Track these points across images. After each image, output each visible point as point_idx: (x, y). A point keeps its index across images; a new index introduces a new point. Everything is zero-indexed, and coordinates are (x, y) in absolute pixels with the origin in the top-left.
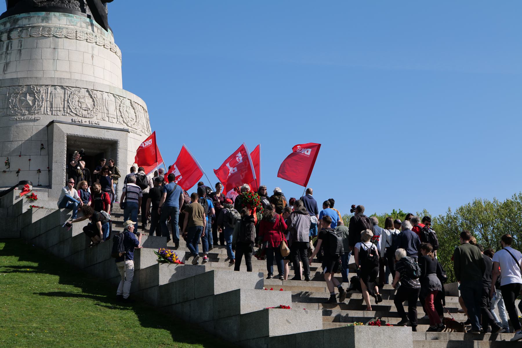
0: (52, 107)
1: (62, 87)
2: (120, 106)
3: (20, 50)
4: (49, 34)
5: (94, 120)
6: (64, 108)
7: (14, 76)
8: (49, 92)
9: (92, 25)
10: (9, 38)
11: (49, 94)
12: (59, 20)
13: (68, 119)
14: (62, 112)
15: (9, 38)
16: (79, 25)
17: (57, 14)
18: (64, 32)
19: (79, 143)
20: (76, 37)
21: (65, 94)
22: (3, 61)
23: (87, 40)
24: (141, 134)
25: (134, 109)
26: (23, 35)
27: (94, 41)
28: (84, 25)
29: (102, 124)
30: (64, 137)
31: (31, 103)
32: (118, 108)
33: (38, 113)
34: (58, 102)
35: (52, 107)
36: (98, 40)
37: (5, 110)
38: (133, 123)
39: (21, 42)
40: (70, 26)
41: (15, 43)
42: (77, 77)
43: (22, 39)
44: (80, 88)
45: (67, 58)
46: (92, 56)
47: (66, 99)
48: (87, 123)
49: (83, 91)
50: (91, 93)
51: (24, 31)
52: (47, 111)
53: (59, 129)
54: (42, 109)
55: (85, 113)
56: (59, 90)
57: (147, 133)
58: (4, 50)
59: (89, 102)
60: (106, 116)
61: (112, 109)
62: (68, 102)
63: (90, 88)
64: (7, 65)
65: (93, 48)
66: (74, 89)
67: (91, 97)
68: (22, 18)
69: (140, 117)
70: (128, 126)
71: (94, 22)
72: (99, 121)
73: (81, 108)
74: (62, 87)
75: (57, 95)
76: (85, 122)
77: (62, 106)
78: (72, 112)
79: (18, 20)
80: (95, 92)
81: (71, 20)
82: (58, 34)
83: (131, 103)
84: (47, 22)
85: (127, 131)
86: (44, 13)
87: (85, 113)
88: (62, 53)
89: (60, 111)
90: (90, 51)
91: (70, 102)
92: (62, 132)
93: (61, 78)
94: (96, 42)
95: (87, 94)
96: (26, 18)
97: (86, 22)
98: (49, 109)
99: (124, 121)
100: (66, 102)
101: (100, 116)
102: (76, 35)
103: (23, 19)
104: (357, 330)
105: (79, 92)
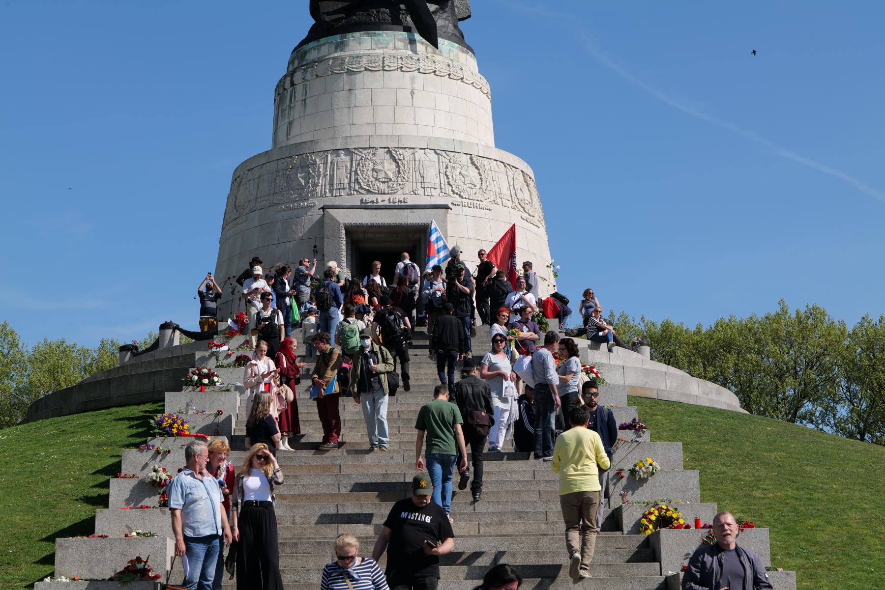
0: (331, 185)
1: (348, 152)
2: (447, 168)
3: (305, 100)
4: (342, 69)
5: (399, 197)
6: (350, 183)
7: (304, 139)
8: (329, 161)
9: (412, 42)
10: (293, 84)
11: (329, 165)
12: (360, 44)
13: (356, 200)
14: (347, 190)
15: (293, 84)
16: (391, 45)
17: (357, 35)
18: (364, 62)
19: (371, 236)
20: (384, 67)
21: (352, 161)
22: (287, 121)
23: (401, 67)
24: (490, 206)
25: (477, 168)
26: (308, 77)
27: (414, 67)
28: (400, 45)
29: (410, 202)
30: (339, 230)
31: (303, 182)
32: (443, 170)
33: (313, 196)
34: (342, 175)
35: (331, 185)
36: (421, 65)
37: (271, 198)
38: (475, 190)
39: (305, 87)
40: (378, 51)
41: (299, 89)
42: (385, 130)
43: (307, 83)
44: (376, 149)
45: (369, 102)
46: (412, 93)
47: (354, 169)
48: (386, 203)
49: (381, 152)
50: (394, 153)
51: (310, 70)
52: (325, 192)
53: (333, 219)
54: (318, 189)
55: (383, 187)
56: (344, 158)
57: (509, 204)
58: (288, 103)
59: (389, 168)
60: (419, 187)
61: (431, 175)
62: (356, 174)
63: (392, 145)
64: (290, 124)
65: (413, 80)
66: (366, 152)
67: (395, 160)
68: (310, 49)
69: (490, 179)
70: (461, 197)
71: (417, 36)
72: (406, 196)
73: (377, 179)
74: (348, 152)
75: (340, 165)
76: (383, 201)
77: (347, 181)
78: (362, 188)
79: (306, 53)
80: (401, 151)
81: (379, 40)
82: (354, 67)
83: (471, 159)
84: (342, 50)
85: (446, 207)
86: (337, 38)
87: (383, 187)
88: (361, 96)
89: (344, 189)
90: (408, 85)
91: (359, 172)
92: (337, 221)
93: (346, 137)
94: (419, 69)
95: (388, 156)
96: (314, 48)
97: (402, 40)
98: (328, 187)
99: (453, 191)
100: (353, 174)
101: (408, 188)
102: (383, 64)
103: (325, 48)
104: (61, 546)
105: (374, 154)
